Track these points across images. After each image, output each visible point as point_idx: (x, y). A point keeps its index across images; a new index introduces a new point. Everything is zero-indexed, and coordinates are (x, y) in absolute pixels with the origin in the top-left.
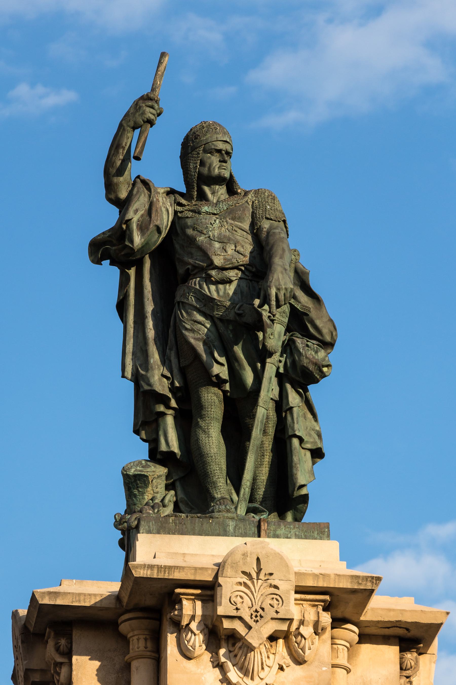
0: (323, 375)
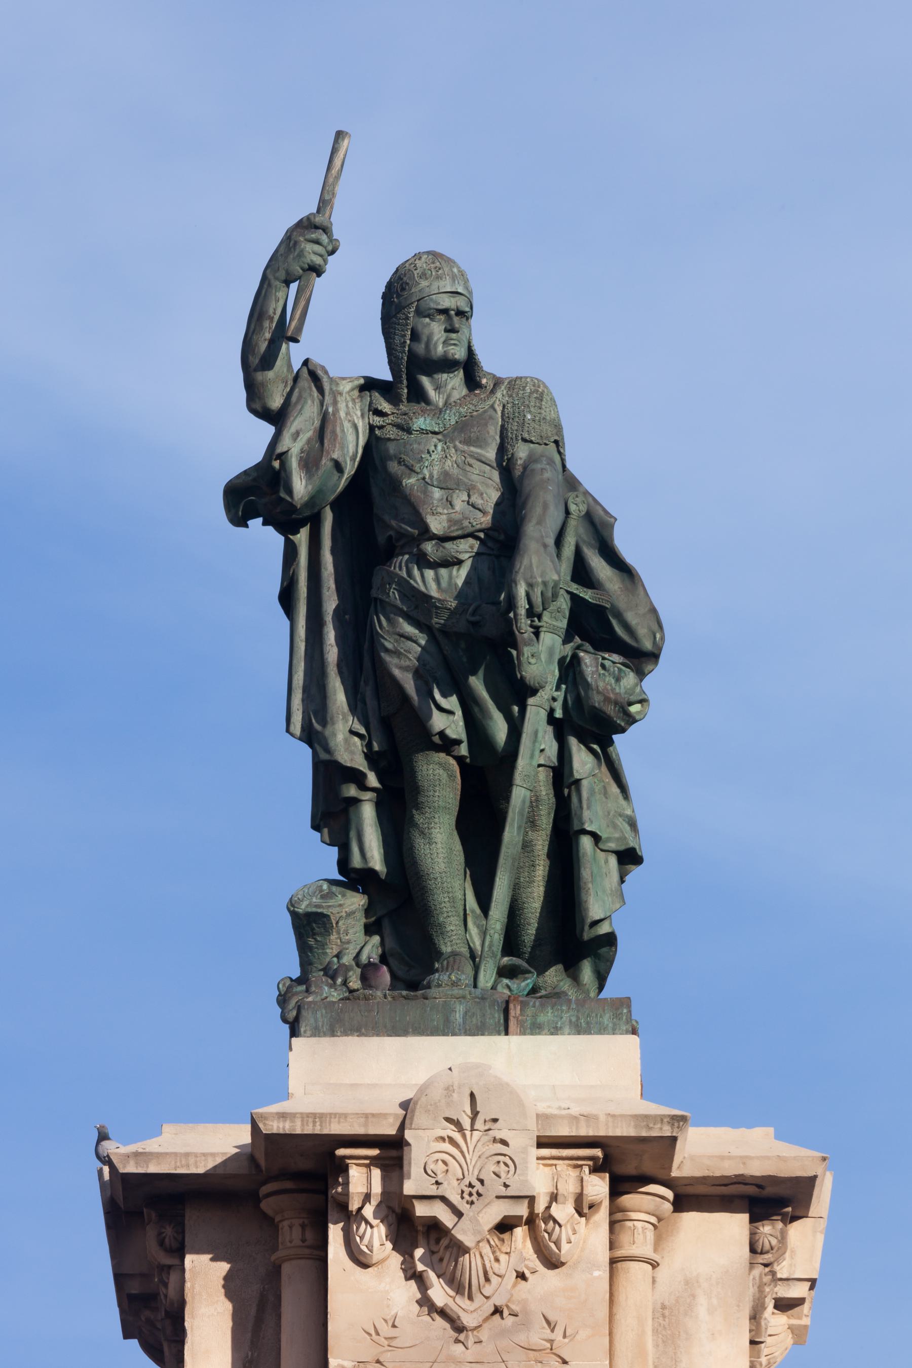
0: (632, 720)
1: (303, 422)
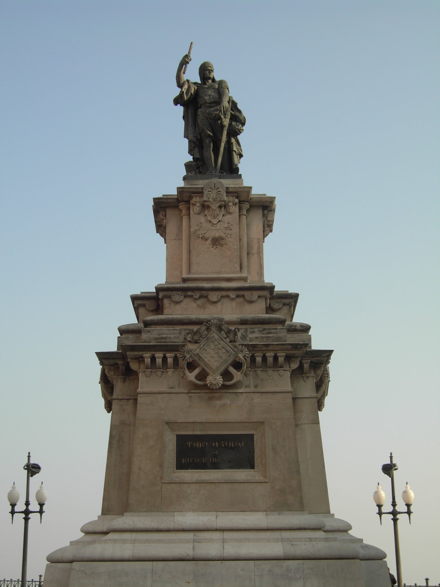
0: (241, 132)
1: (186, 87)
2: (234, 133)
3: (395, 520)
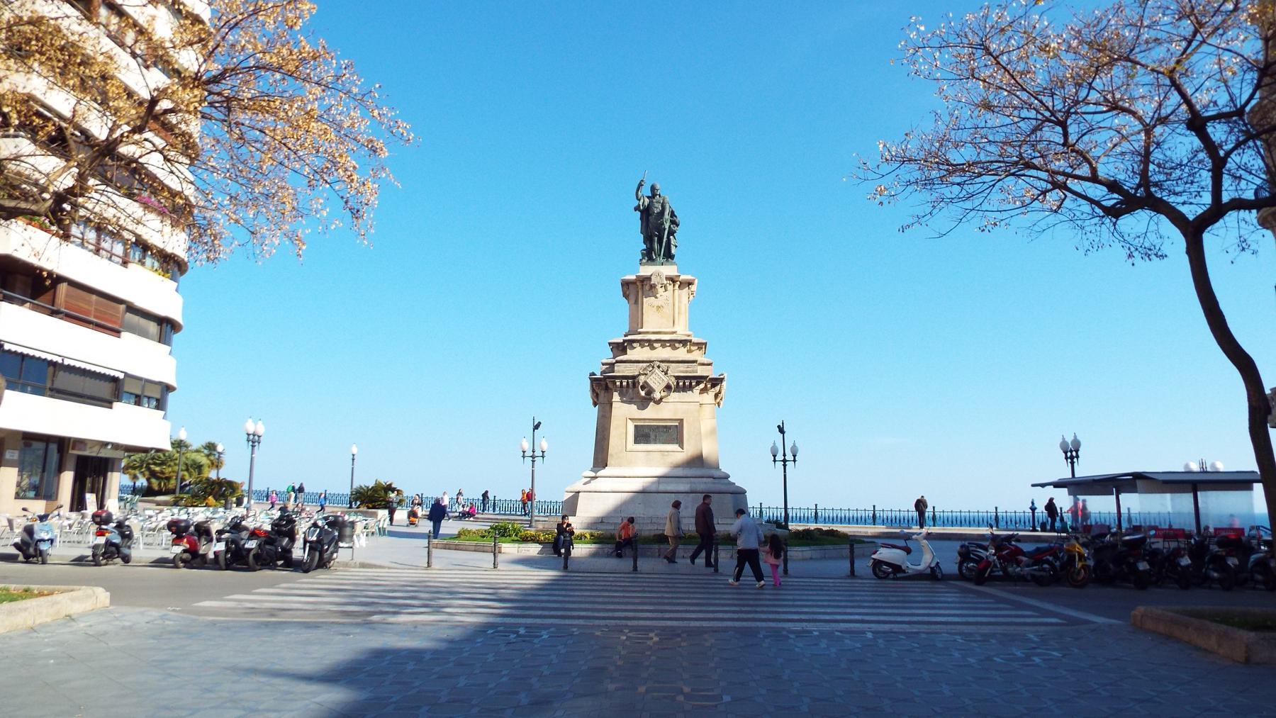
2: (671, 233)
3: (785, 466)
